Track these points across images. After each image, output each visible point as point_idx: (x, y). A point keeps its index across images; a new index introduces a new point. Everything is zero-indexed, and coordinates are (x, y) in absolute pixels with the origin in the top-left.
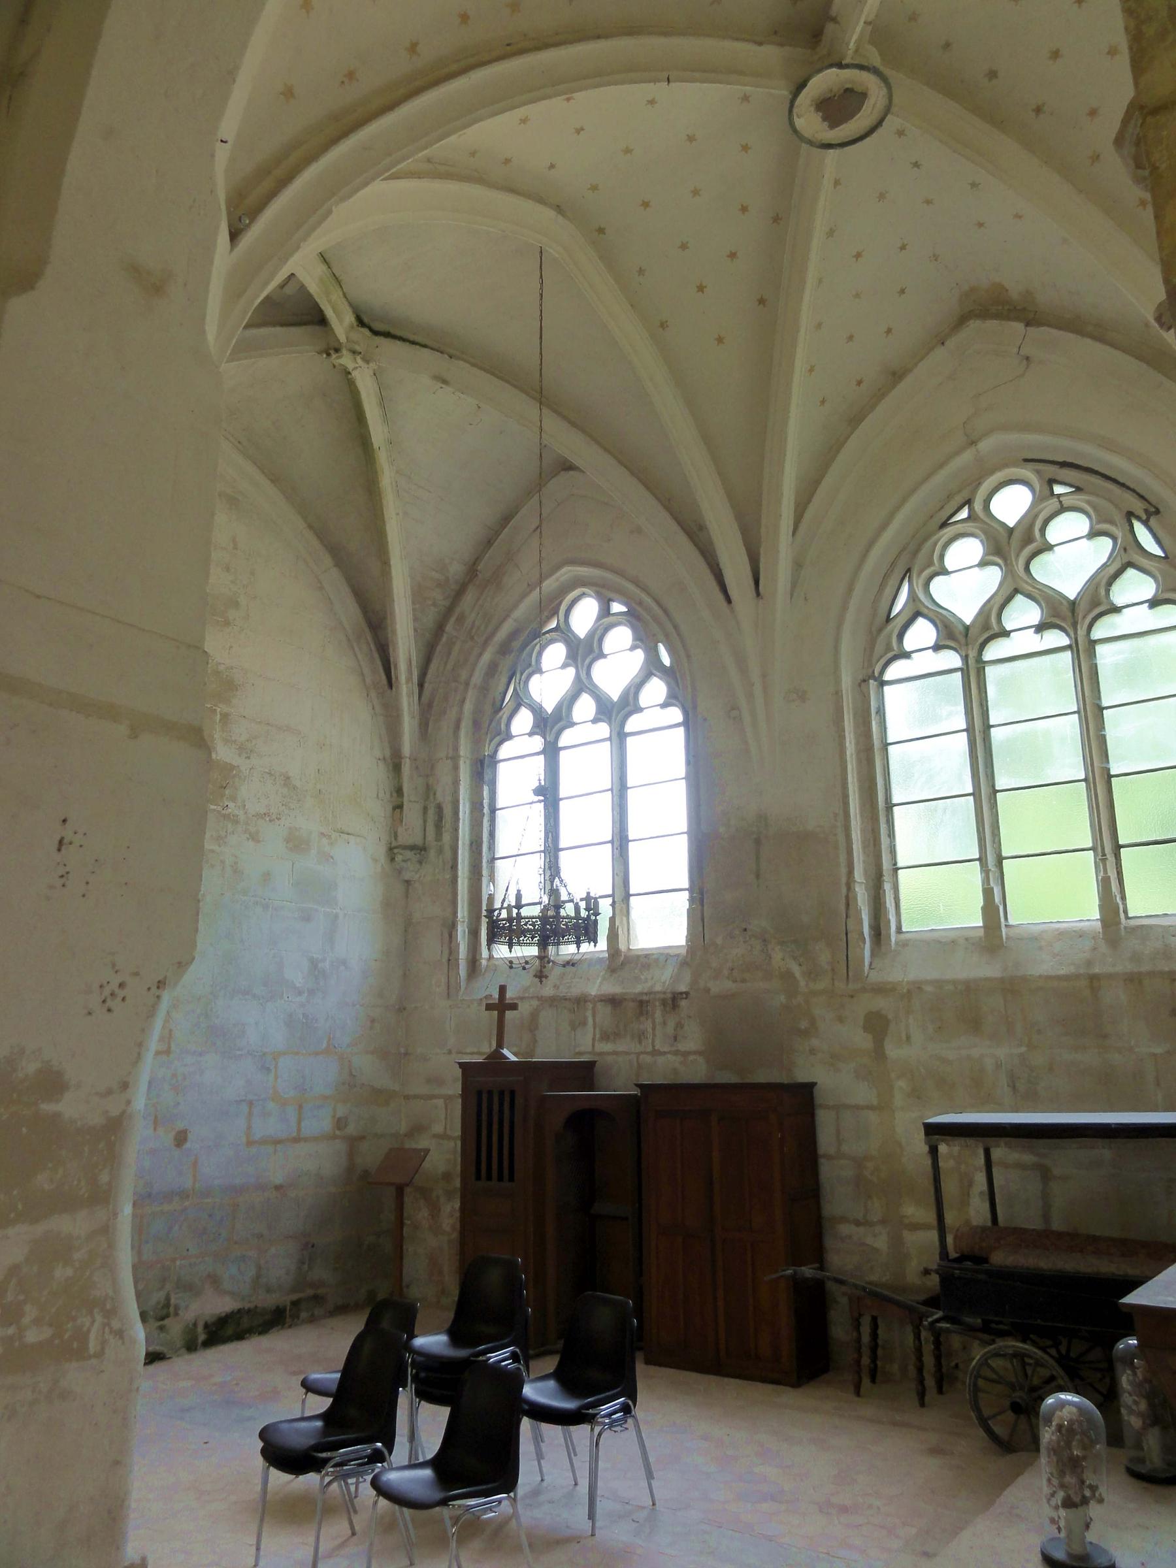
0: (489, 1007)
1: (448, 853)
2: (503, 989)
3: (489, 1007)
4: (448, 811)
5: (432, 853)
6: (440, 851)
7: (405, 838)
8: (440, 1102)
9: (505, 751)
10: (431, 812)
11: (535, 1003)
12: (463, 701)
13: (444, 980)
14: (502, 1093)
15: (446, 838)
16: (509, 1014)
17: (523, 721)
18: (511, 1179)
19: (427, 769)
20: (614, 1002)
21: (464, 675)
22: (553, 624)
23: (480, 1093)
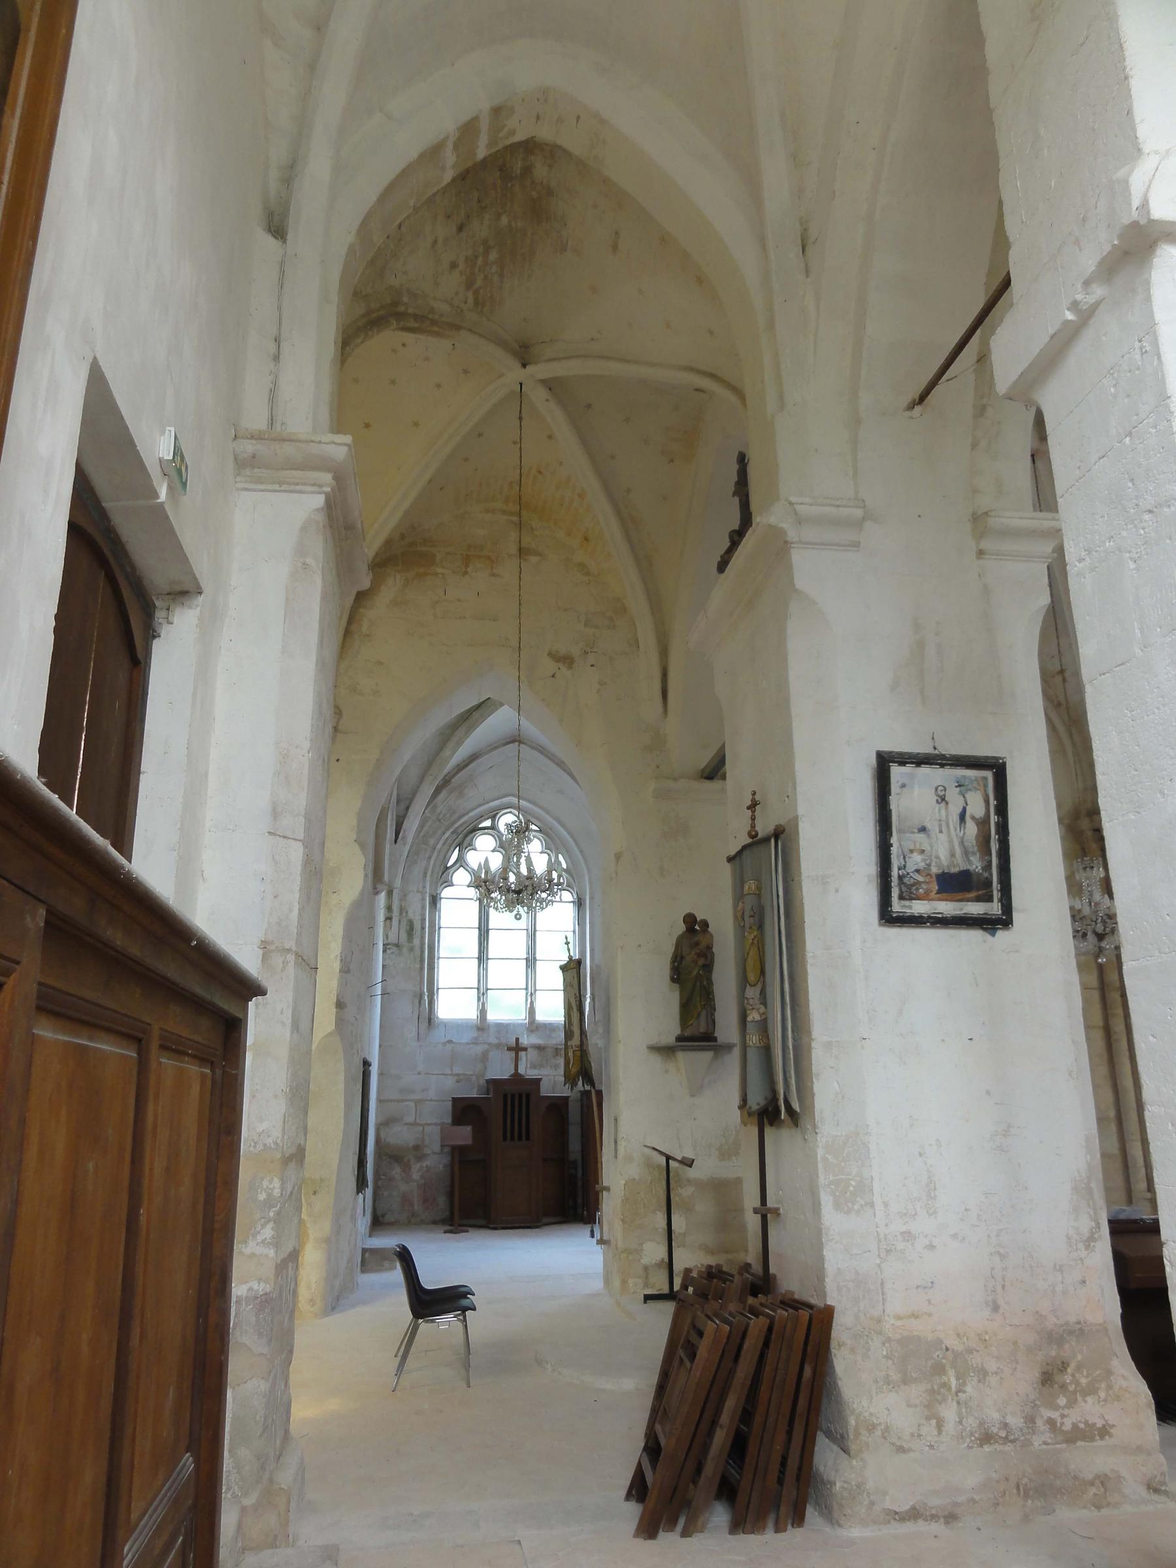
0: (509, 1049)
1: (418, 952)
2: (517, 1039)
3: (509, 1049)
4: (417, 926)
5: (405, 950)
6: (412, 949)
7: (393, 938)
8: (412, 1104)
9: (446, 892)
10: (404, 923)
11: (486, 1047)
12: (430, 858)
13: (415, 1029)
14: (520, 1096)
15: (416, 942)
16: (522, 1054)
17: (461, 877)
18: (528, 1138)
19: (404, 897)
20: (540, 1048)
21: (432, 842)
22: (488, 823)
23: (505, 1096)
